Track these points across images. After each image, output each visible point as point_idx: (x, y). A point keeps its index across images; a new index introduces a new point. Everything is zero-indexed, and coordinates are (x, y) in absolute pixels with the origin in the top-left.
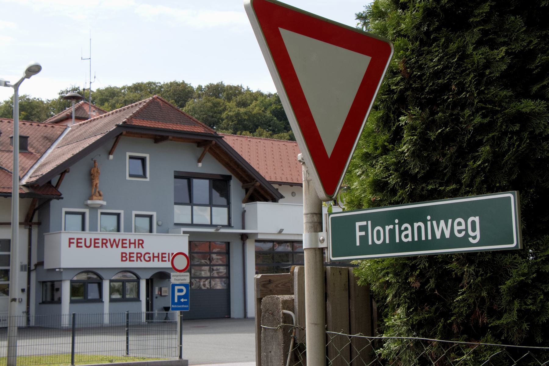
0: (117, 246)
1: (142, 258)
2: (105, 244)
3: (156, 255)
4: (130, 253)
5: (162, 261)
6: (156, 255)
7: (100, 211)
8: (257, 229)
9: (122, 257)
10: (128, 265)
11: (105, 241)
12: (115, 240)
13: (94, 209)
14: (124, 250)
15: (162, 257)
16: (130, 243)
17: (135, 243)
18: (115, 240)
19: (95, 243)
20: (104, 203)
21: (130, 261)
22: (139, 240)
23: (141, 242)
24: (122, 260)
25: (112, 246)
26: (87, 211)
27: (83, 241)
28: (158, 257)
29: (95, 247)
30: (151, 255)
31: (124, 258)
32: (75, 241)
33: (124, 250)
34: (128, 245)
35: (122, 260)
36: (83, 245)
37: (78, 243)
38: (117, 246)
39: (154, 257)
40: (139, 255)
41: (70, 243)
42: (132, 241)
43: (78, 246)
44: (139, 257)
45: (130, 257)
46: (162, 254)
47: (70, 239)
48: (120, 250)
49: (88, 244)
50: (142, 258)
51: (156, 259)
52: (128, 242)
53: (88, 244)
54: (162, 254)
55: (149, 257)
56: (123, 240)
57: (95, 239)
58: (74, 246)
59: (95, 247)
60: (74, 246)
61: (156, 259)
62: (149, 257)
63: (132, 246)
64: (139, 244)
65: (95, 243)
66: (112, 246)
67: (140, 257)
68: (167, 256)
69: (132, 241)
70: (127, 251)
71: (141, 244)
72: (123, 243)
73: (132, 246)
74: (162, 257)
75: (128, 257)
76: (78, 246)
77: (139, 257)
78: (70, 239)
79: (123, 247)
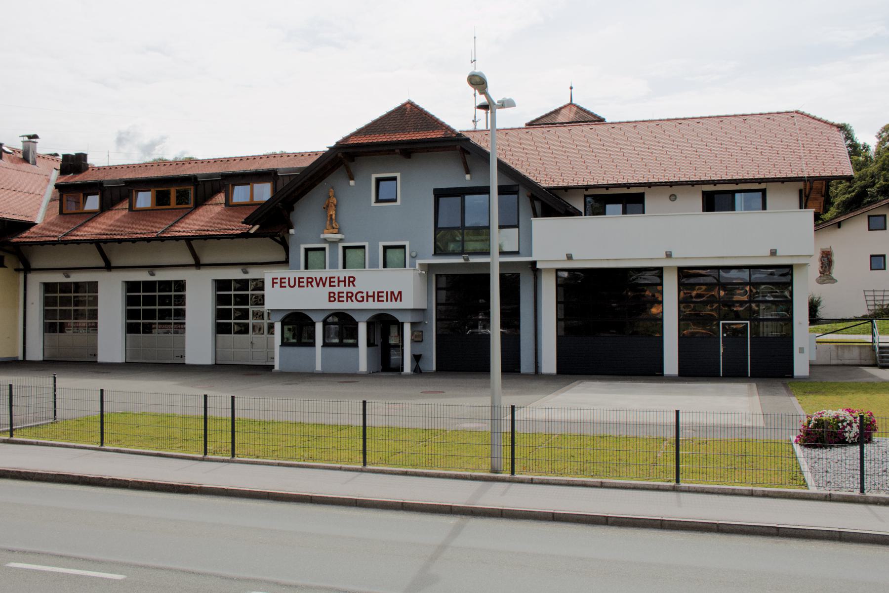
0: (324, 285)
1: (353, 298)
2: (311, 283)
3: (371, 294)
4: (339, 293)
5: (379, 301)
6: (371, 294)
7: (341, 245)
8: (531, 255)
9: (330, 297)
10: (336, 306)
11: (310, 280)
12: (321, 279)
13: (334, 243)
14: (332, 289)
15: (379, 296)
16: (339, 281)
17: (344, 281)
18: (321, 279)
19: (299, 282)
20: (339, 236)
21: (339, 301)
22: (349, 278)
23: (352, 279)
24: (330, 301)
25: (318, 285)
26: (326, 246)
27: (287, 281)
28: (373, 296)
29: (299, 286)
30: (365, 295)
31: (331, 297)
32: (278, 281)
33: (332, 289)
34: (336, 284)
35: (330, 301)
36: (287, 284)
37: (281, 282)
38: (324, 285)
39: (368, 296)
40: (350, 295)
41: (273, 283)
42: (342, 279)
43: (281, 286)
44: (350, 296)
45: (339, 297)
46: (379, 293)
47: (273, 279)
48: (327, 289)
49: (292, 284)
50: (353, 298)
51: (371, 299)
52: (336, 280)
53: (292, 284)
54: (379, 293)
55: (363, 297)
56: (330, 278)
57: (299, 278)
58: (277, 286)
59: (299, 286)
60: (277, 286)
61: (371, 299)
62: (363, 297)
63: (342, 284)
64: (349, 282)
65: (299, 282)
66: (318, 285)
67: (351, 297)
68: (384, 295)
69: (342, 279)
70: (336, 290)
71: (353, 282)
72: (330, 282)
73: (342, 284)
74: (378, 296)
75: (336, 296)
76: (281, 286)
77: (350, 296)
78: (273, 279)
79: (330, 286)
